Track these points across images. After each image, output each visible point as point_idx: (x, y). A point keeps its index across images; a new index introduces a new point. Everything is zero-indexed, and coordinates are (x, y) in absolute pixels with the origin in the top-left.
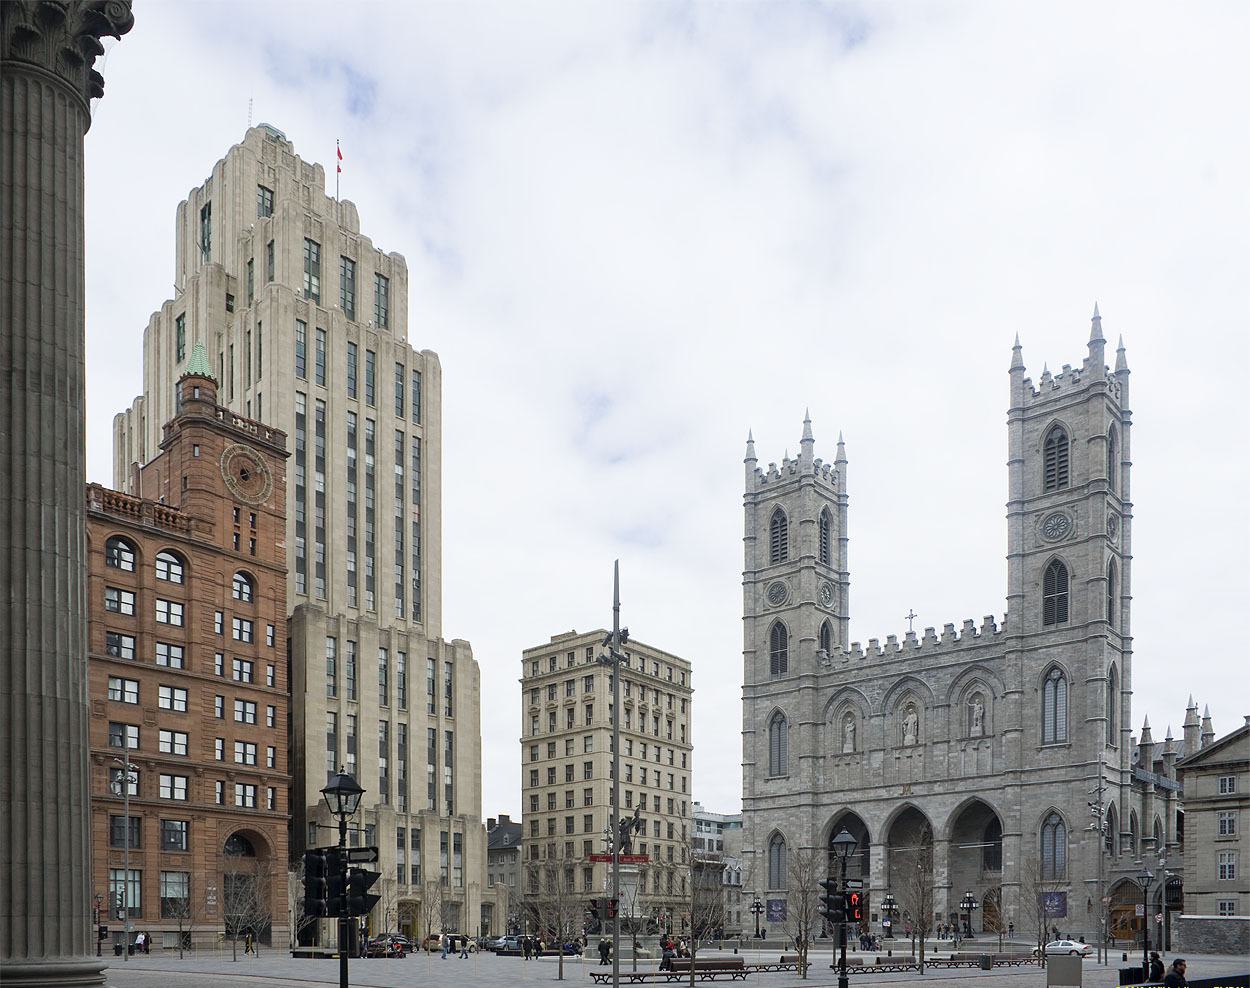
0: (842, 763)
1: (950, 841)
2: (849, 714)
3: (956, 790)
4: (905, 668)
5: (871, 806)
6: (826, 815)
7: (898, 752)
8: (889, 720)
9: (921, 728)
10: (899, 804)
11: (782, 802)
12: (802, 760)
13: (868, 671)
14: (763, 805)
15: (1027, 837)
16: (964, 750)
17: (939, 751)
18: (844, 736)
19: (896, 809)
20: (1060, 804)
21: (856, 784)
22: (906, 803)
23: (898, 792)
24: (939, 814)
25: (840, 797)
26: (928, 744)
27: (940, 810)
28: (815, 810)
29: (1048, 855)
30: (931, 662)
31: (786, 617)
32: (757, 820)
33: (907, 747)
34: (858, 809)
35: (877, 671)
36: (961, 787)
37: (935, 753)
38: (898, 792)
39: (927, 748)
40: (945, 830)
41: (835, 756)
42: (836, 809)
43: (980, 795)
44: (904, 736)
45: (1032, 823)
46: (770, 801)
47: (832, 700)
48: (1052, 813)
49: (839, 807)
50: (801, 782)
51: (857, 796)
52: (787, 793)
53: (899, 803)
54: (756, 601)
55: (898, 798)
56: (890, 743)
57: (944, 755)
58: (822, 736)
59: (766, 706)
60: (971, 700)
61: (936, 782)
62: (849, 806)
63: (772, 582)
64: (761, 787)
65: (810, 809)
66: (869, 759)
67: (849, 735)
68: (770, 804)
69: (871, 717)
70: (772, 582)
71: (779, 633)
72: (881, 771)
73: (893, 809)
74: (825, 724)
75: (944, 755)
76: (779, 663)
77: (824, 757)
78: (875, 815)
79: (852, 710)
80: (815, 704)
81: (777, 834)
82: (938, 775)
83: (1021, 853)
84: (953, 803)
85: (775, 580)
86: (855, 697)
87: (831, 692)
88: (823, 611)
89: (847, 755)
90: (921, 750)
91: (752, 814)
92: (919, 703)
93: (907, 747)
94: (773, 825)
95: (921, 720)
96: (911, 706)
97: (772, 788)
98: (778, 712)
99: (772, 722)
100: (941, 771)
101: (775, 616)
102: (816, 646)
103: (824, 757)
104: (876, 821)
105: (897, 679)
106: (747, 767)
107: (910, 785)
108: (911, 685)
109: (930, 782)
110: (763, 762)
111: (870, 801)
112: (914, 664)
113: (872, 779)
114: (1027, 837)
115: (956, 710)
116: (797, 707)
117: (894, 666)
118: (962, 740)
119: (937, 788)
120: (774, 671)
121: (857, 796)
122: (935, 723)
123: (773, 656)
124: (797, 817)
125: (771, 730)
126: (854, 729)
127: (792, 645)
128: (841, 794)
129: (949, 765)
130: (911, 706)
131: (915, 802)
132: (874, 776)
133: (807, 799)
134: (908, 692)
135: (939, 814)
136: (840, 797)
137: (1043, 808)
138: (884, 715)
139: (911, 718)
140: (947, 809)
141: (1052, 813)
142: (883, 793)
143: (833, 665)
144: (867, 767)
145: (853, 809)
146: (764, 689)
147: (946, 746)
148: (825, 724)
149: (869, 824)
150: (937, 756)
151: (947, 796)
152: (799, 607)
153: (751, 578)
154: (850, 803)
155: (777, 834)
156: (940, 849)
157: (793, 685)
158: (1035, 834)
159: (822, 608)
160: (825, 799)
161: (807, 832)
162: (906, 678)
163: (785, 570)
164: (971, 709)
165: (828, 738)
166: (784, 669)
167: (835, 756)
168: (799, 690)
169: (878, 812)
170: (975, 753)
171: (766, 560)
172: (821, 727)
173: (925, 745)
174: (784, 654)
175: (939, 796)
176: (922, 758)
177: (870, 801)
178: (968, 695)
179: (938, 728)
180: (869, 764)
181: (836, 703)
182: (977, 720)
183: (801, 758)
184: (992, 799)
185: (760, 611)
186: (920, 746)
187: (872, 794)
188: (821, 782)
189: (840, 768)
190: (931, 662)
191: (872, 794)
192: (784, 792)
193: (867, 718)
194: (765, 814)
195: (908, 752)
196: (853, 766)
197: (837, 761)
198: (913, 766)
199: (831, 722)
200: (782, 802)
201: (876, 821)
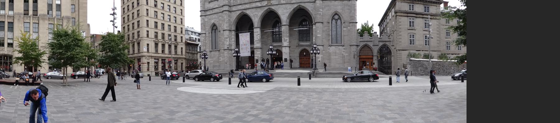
5: (254, 10)
6: (235, 16)
11: (216, 11)
14: (208, 13)
15: (325, 24)
20: (339, 10)
24: (284, 14)
25: (240, 7)
27: (285, 11)
29: (334, 33)
34: (248, 12)
43: (303, 4)
45: (328, 18)
46: (211, 11)
48: (336, 14)
49: (240, 12)
51: (247, 6)
53: (266, 8)
62: (244, 11)
65: (227, 12)
68: (211, 12)
81: (214, 25)
83: (323, 31)
91: (204, 17)
94: (213, 21)
97: (212, 5)
104: (256, 17)
111: (253, 8)
114: (325, 24)
121: (247, 6)
124: (222, 17)
128: (240, 6)
131: (273, 8)
133: (226, 8)
135: (284, 14)
136: (240, 7)
137: (332, 12)
141: (336, 14)
142: (259, 4)
149: (253, 18)
154: (245, 9)
155: (214, 25)
156: (285, 29)
158: (329, 23)
160: (234, 9)
161: (227, 23)
177: (253, 8)
184: (309, 7)
187: (254, 5)
191: (254, 5)
194: (209, 17)
200: (216, 11)
201: (256, 17)
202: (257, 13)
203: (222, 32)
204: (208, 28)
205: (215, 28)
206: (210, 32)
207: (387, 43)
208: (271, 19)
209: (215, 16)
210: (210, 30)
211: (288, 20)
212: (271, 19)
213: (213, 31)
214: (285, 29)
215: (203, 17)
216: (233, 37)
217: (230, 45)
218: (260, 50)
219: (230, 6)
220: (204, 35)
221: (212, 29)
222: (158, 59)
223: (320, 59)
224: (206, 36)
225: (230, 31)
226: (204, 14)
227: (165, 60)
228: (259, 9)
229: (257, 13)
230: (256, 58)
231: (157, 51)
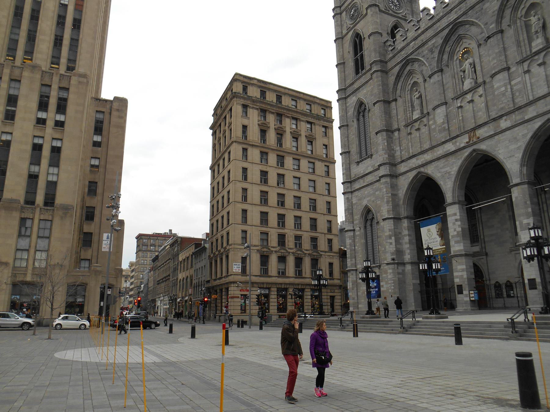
1: (529, 183)
3: (526, 118)
4: (453, 17)
5: (441, 163)
6: (404, 183)
7: (459, 101)
8: (447, 77)
9: (478, 68)
10: (466, 154)
12: (378, 135)
14: (357, 186)
16: (528, 71)
17: (499, 83)
18: (413, 106)
19: (466, 159)
21: (426, 146)
22: (474, 150)
23: (463, 140)
25: (414, 162)
26: (487, 81)
27: (513, 147)
28: (394, 180)
32: (354, 201)
34: (431, 171)
36: (531, 112)
37: (495, 87)
38: (463, 140)
39: (487, 86)
40: (521, 170)
42: (411, 175)
44: (463, 83)
46: (361, 181)
47: (399, 76)
49: (414, 173)
51: (427, 157)
52: (372, 169)
54: (342, 26)
55: (464, 148)
56: (450, 94)
57: (505, 85)
58: (395, 111)
59: (352, 101)
60: (527, 14)
61: (501, 117)
62: (422, 169)
66: (434, 118)
67: (416, 103)
69: (430, 77)
71: (358, 43)
72: (446, 125)
73: (460, 162)
74: (396, 100)
75: (505, 85)
76: (359, 65)
78: (446, 173)
79: (415, 80)
80: (385, 85)
82: (502, 109)
84: (524, 136)
86: (416, 65)
88: (391, 15)
89: (416, 121)
90: (481, 90)
91: (349, 196)
92: (473, 45)
94: (365, 202)
95: (477, 61)
96: (467, 52)
99: (359, 113)
100: (505, 104)
102: (386, 37)
103: (399, 130)
104: (447, 177)
107: (474, 129)
108: (461, 31)
109: (494, 120)
110: (354, 149)
111: (438, 159)
112: (460, 9)
115: (510, 33)
118: (523, 61)
119: (504, 124)
120: (357, 72)
121: (427, 157)
122: (489, 57)
123: (356, 62)
125: (358, 120)
126: (420, 97)
128: (414, 160)
129: (513, 94)
130: (467, 52)
131: (483, 146)
132: (440, 131)
136: (414, 162)
138: (441, 71)
139: (466, 65)
140: (519, 144)
142: (450, 147)
143: (396, 47)
144: (433, 127)
145: (426, 171)
147: (505, 74)
148: (396, 100)
149: (441, 183)
150: (499, 88)
151: (516, 129)
153: (338, 11)
154: (423, 165)
159: (391, 12)
160: (402, 168)
162: (456, 26)
164: (528, 26)
165: (399, 110)
167: (406, 126)
169: (449, 168)
170: (541, 70)
172: (394, 103)
173: (484, 82)
174: (362, 56)
175: (508, 132)
176: (483, 99)
177: (438, 159)
178: (521, 12)
179: (493, 59)
180: (435, 122)
182: (537, 32)
187: (440, 151)
188: (398, 153)
189: (413, 136)
191: (440, 151)
192: (370, 169)
195: (469, 97)
198: (476, 109)
199: (400, 96)
200: (370, 179)
201: (447, 177)
202: (447, 169)
203: (382, 223)
204: (357, 217)
205: (370, 217)
208: (483, 175)
209: (368, 190)
210: (362, 221)
211: (525, 170)
212: (483, 175)
213: (369, 223)
214: (519, 195)
215: (347, 196)
216: (406, 232)
217: (399, 252)
218: (463, 260)
219: (393, 165)
220: (351, 234)
221: (366, 220)
222: (269, 289)
224: (354, 236)
225: (397, 219)
227: (286, 290)
228: (451, 159)
229: (447, 169)
230: (457, 281)
231: (265, 272)
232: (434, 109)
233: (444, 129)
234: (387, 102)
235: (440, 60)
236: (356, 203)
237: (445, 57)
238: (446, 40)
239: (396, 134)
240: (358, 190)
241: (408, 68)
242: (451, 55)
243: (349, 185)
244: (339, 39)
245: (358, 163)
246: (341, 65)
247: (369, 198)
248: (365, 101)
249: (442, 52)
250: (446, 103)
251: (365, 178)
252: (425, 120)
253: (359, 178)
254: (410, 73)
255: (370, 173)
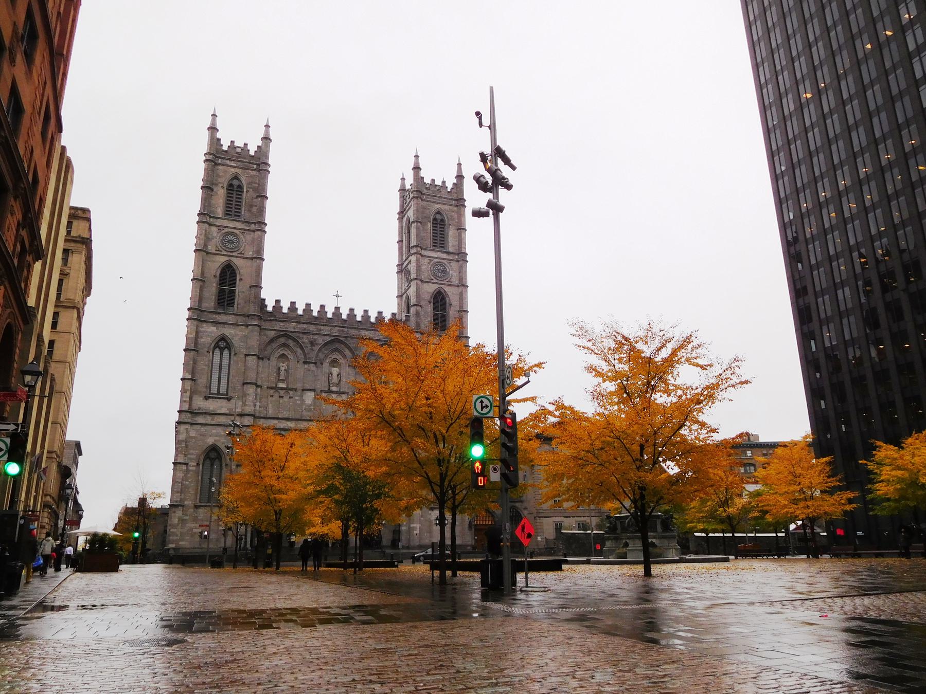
0: (276, 395)
2: (283, 355)
9: (344, 380)
13: (305, 326)
14: (200, 420)
30: (353, 332)
31: (238, 262)
33: (333, 392)
35: (312, 328)
41: (271, 388)
47: (272, 341)
50: (244, 404)
59: (211, 332)
63: (226, 230)
64: (200, 403)
68: (209, 420)
69: (305, 363)
70: (226, 230)
71: (228, 274)
77: (260, 387)
85: (230, 230)
86: (291, 343)
87: (272, 334)
89: (282, 389)
92: (342, 361)
93: (333, 392)
94: (210, 441)
98: (223, 338)
101: (226, 258)
105: (329, 339)
106: (189, 383)
108: (337, 345)
113: (305, 413)
116: (245, 338)
117: (327, 328)
123: (221, 293)
127: (241, 288)
128: (276, 421)
130: (334, 363)
134: (336, 350)
138: (315, 363)
139: (335, 371)
146: (210, 315)
152: (252, 259)
155: (214, 449)
157: (240, 320)
163: (238, 225)
166: (231, 303)
167: (271, 388)
168: (247, 326)
171: (220, 211)
174: (232, 292)
180: (303, 401)
181: (274, 345)
183: (244, 384)
185: (211, 248)
186: (344, 393)
188: (257, 408)
190: (353, 332)
192: (224, 411)
193: (301, 362)
194: (203, 429)
196: (286, 399)
197: (272, 392)
206: (201, 462)
207: (517, 505)
210: (202, 457)
220: (184, 467)
223: (417, 532)
224: (187, 471)
226: (187, 418)
232: (303, 390)
233: (310, 410)
234: (259, 358)
235: (317, 355)
236: (194, 437)
237: (321, 356)
238: (326, 344)
239: (259, 390)
240: (201, 424)
241: (282, 340)
242: (326, 357)
243: (189, 415)
244: (202, 251)
245: (206, 398)
246: (199, 280)
247: (217, 438)
248: (236, 342)
249: (320, 350)
250: (314, 390)
251: (216, 417)
252: (291, 392)
253: (206, 413)
254: (284, 345)
255: (226, 414)
